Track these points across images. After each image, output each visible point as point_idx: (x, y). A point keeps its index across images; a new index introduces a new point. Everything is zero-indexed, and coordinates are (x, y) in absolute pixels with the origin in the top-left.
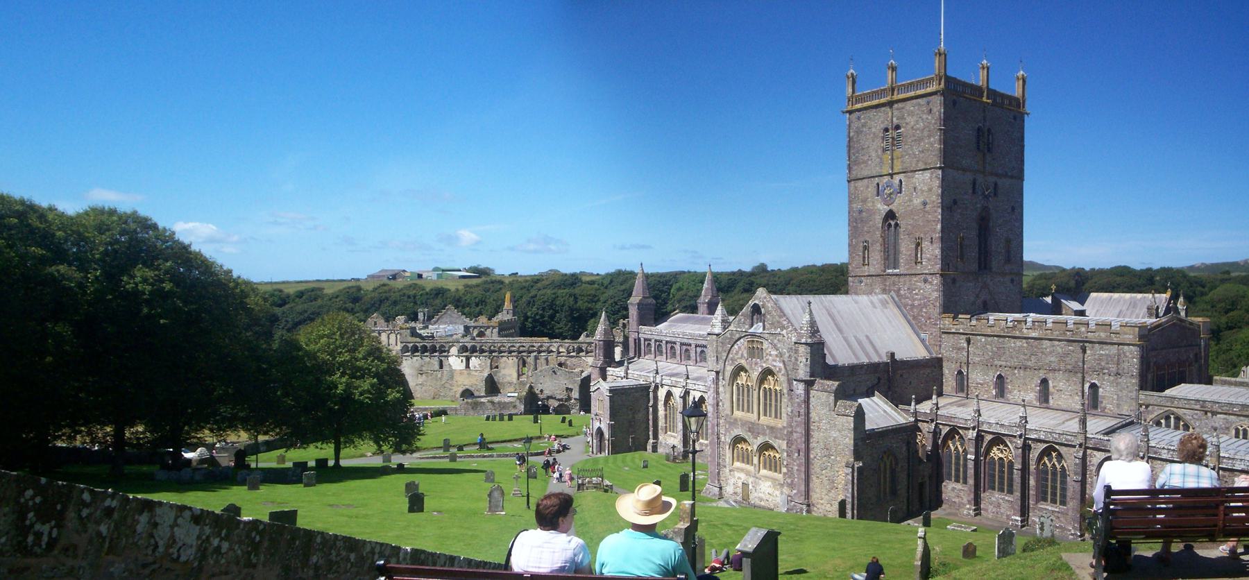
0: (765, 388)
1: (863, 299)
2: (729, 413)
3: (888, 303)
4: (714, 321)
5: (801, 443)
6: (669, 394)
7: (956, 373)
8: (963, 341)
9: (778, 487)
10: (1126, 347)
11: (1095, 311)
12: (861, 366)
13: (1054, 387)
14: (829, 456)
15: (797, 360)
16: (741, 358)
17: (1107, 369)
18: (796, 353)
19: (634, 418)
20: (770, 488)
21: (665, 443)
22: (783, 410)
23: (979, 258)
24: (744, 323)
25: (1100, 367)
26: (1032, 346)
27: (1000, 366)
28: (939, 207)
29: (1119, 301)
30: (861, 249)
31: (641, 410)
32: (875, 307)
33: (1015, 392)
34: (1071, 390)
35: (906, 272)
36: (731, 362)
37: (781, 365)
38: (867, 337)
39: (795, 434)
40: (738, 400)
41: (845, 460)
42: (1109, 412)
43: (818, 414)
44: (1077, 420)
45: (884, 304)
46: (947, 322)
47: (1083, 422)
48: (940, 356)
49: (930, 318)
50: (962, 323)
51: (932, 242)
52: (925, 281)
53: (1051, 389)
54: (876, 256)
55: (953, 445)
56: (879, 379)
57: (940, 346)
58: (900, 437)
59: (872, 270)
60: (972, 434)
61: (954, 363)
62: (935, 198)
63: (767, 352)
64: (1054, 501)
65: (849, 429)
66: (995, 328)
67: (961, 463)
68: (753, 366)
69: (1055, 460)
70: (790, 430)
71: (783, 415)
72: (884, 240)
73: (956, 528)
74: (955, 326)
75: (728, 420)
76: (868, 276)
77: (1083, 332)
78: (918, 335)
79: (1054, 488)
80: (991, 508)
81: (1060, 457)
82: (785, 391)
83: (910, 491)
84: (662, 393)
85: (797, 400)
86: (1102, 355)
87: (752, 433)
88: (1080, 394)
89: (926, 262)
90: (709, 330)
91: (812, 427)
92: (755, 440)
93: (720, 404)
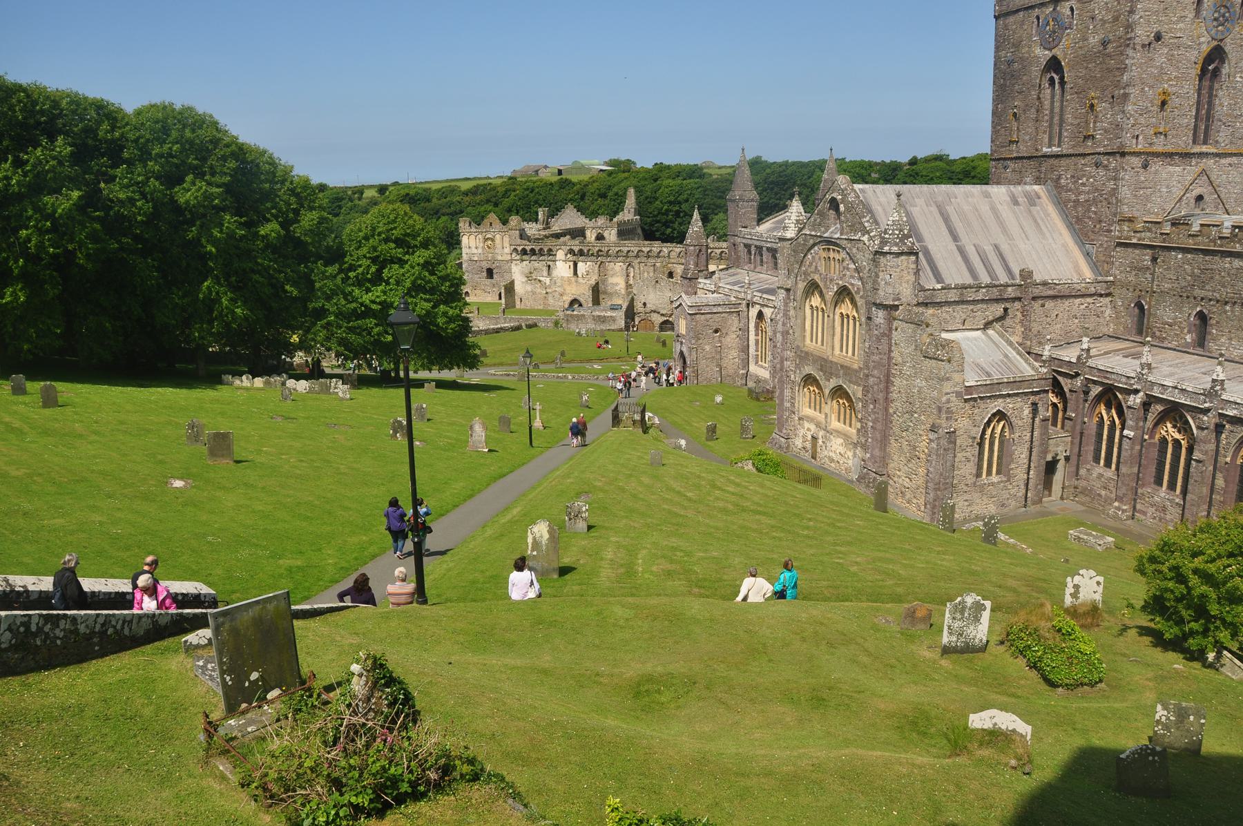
0: (841, 313)
1: (998, 192)
3: (1039, 198)
4: (787, 221)
6: (760, 315)
7: (1133, 305)
14: (911, 413)
15: (877, 276)
16: (815, 273)
20: (841, 448)
24: (820, 225)
27: (1202, 299)
32: (1016, 203)
35: (1071, 151)
36: (803, 277)
38: (996, 247)
39: (871, 380)
41: (931, 421)
43: (901, 354)
45: (1032, 200)
46: (1126, 228)
48: (1112, 278)
49: (1100, 221)
50: (1150, 230)
52: (1097, 165)
55: (1108, 414)
56: (1006, 310)
59: (1024, 150)
61: (1131, 290)
63: (845, 264)
66: (1200, 238)
67: (1117, 440)
73: (1081, 536)
74: (1138, 235)
75: (799, 353)
76: (1016, 158)
80: (1151, 510)
83: (1031, 473)
84: (753, 312)
85: (876, 332)
87: (825, 373)
89: (1100, 134)
90: (780, 234)
91: (894, 371)
92: (827, 383)
93: (791, 331)
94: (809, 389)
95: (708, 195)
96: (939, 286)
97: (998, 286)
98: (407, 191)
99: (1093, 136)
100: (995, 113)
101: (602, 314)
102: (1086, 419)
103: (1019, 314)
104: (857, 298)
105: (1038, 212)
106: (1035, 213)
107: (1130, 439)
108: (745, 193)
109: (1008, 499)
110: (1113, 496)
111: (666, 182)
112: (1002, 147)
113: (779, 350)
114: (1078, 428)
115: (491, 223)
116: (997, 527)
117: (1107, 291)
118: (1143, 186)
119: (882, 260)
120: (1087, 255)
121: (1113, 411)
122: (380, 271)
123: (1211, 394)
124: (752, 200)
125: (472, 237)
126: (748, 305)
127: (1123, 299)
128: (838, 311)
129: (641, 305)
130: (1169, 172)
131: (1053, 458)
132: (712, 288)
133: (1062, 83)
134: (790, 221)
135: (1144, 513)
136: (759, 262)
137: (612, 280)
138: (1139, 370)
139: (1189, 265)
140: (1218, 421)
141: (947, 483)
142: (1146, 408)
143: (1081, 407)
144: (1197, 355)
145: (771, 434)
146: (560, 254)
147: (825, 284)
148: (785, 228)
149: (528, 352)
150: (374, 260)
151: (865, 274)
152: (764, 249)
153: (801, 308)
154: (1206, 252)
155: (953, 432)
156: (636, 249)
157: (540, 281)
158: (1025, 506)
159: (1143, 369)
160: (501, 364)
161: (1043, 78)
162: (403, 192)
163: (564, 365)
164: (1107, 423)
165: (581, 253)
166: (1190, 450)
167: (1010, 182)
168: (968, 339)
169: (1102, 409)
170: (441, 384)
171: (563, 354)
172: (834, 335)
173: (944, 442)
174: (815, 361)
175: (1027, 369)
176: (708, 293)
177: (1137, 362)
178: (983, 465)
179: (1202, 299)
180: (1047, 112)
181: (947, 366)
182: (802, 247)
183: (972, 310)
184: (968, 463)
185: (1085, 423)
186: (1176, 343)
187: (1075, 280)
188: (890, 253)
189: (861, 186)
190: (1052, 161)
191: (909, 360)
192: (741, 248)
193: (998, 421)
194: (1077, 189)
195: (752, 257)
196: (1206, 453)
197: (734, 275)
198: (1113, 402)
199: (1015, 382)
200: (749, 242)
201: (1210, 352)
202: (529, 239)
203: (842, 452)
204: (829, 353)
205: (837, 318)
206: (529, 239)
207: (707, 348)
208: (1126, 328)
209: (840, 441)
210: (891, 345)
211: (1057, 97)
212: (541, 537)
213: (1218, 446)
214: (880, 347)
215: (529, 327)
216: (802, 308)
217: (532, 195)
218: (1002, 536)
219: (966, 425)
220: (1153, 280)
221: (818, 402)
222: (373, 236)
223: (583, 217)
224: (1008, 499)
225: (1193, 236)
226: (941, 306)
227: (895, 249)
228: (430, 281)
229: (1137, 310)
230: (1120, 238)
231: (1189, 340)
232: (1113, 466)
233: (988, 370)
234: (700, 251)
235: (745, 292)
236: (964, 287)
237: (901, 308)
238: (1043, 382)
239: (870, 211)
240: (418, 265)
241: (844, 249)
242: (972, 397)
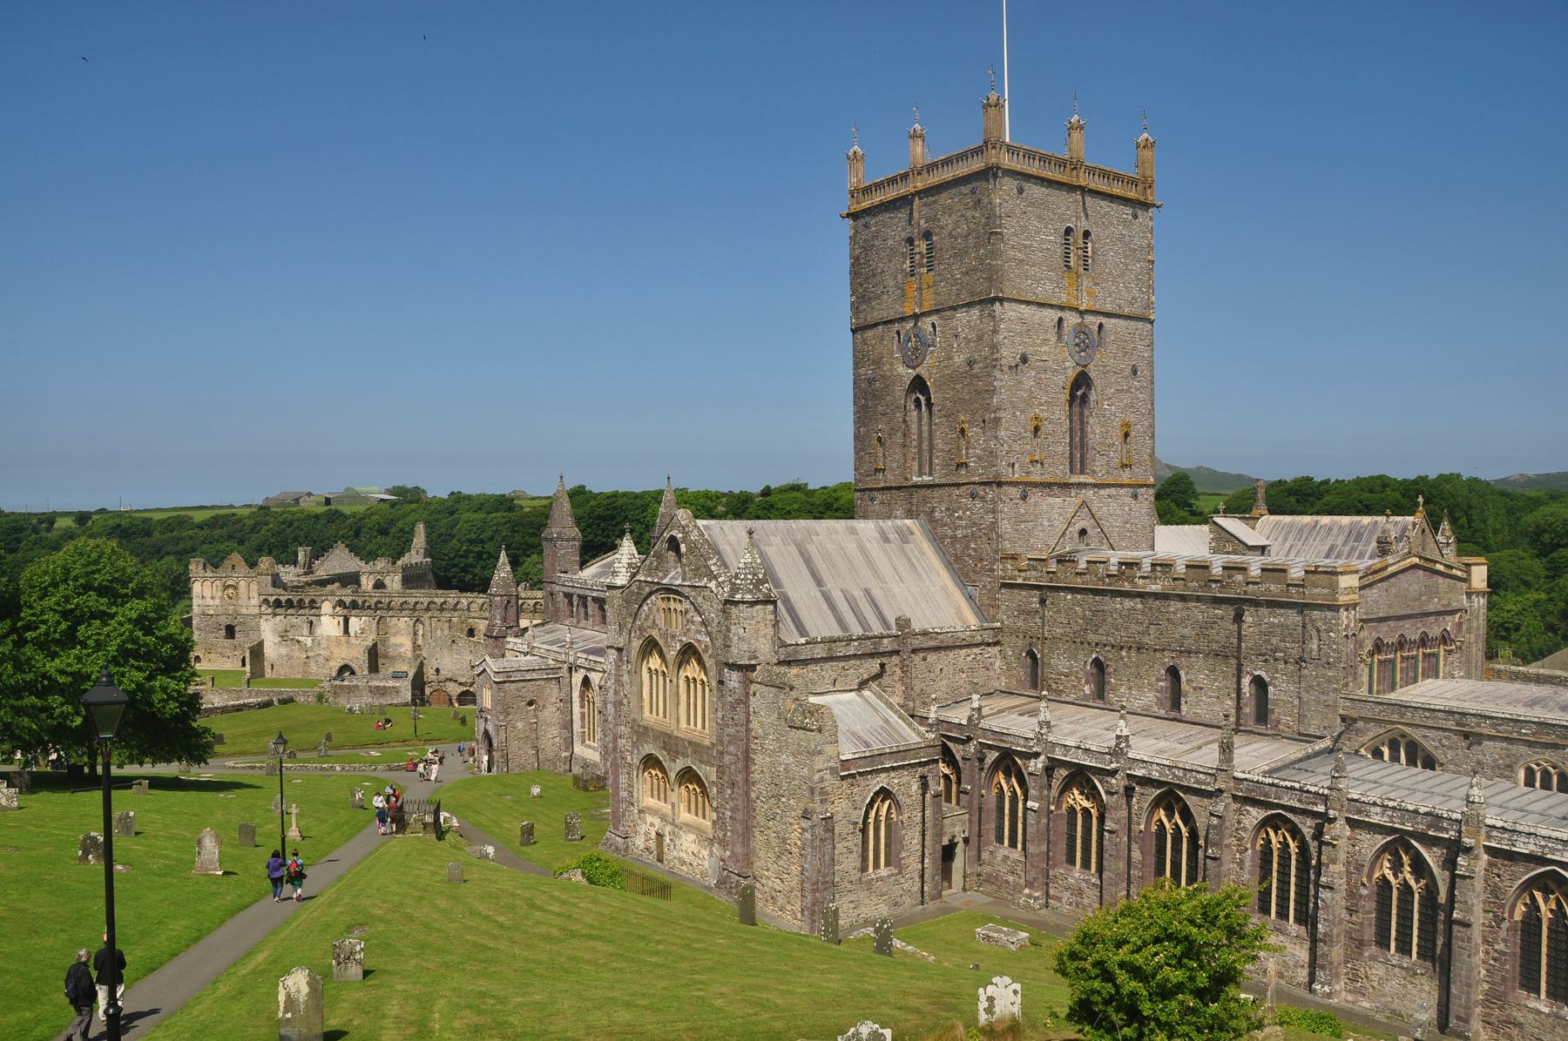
0: (687, 677)
1: (865, 527)
3: (912, 533)
4: (616, 565)
6: (586, 682)
7: (1024, 655)
11: (1287, 545)
13: (1187, 680)
14: (778, 797)
15: (729, 630)
16: (652, 628)
19: (536, 716)
24: (657, 569)
26: (1151, 609)
27: (1097, 644)
28: (995, 366)
29: (1330, 529)
32: (886, 540)
33: (1122, 690)
34: (1219, 689)
35: (943, 481)
36: (638, 632)
38: (867, 592)
39: (727, 759)
40: (651, 694)
44: (1216, 746)
45: (905, 536)
47: (1226, 749)
48: (999, 624)
49: (981, 560)
50: (1035, 569)
52: (973, 496)
53: (1184, 686)
55: (1008, 783)
56: (882, 666)
59: (891, 479)
60: (1037, 765)
61: (1021, 637)
63: (688, 616)
67: (1020, 814)
69: (1177, 816)
73: (991, 934)
74: (1023, 574)
75: (636, 728)
76: (884, 489)
77: (1239, 583)
80: (1066, 895)
81: (1187, 816)
83: (926, 861)
84: (577, 678)
85: (730, 699)
86: (1272, 625)
88: (1234, 695)
89: (974, 462)
90: (608, 581)
91: (753, 746)
93: (625, 701)
94: (650, 773)
95: (518, 531)
96: (803, 640)
97: (871, 638)
98: (117, 521)
99: (966, 463)
100: (857, 437)
101: (382, 684)
102: (983, 792)
103: (898, 671)
104: (705, 657)
105: (912, 550)
106: (908, 551)
107: (1035, 811)
108: (565, 529)
109: (901, 896)
110: (1022, 881)
111: (465, 516)
112: (867, 476)
113: (611, 726)
114: (976, 802)
115: (234, 566)
116: (891, 933)
117: (995, 639)
118: (1024, 519)
119: (734, 610)
120: (970, 598)
121: (1013, 780)
122: (73, 629)
123: (1116, 752)
124: (574, 539)
125: (208, 584)
126: (570, 669)
127: (1013, 647)
128: (682, 674)
129: (433, 671)
132: (525, 648)
133: (929, 405)
134: (621, 565)
135: (1059, 899)
136: (583, 615)
137: (394, 640)
138: (1037, 730)
139: (1079, 606)
140: (1127, 783)
141: (827, 882)
142: (1049, 773)
143: (977, 776)
144: (1098, 708)
145: (605, 833)
146: (327, 607)
147: (666, 642)
148: (615, 574)
149: (281, 736)
150: (65, 615)
151: (713, 628)
152: (589, 599)
153: (637, 672)
154: (1096, 592)
155: (829, 818)
156: (426, 601)
157: (298, 642)
158: (922, 903)
160: (243, 753)
161: (908, 399)
162: (111, 522)
163: (330, 753)
164: (1008, 794)
165: (354, 605)
166: (1101, 819)
167: (878, 517)
168: (840, 702)
169: (1001, 777)
170: (157, 783)
171: (329, 737)
172: (678, 704)
173: (819, 831)
174: (656, 738)
175: (911, 735)
176: (519, 654)
177: (1035, 720)
178: (868, 856)
179: (1097, 644)
180: (915, 437)
181: (817, 736)
182: (636, 597)
183: (843, 668)
184: (850, 856)
185: (983, 796)
186: (1074, 696)
187: (959, 628)
188: (744, 602)
189: (705, 522)
190: (923, 492)
191: (772, 731)
192: (561, 597)
193: (883, 801)
194: (954, 523)
195: (575, 609)
196: (1118, 822)
197: (552, 632)
198: (1013, 769)
199: (899, 752)
200: (571, 590)
202: (284, 587)
204: (674, 727)
205: (682, 682)
206: (284, 587)
207: (520, 725)
208: (1019, 681)
209: (692, 837)
210: (749, 714)
211: (925, 420)
212: (298, 991)
213: (1130, 813)
214: (736, 717)
215: (283, 702)
216: (638, 671)
217: (289, 530)
218: (898, 943)
219: (845, 807)
220: (1043, 626)
221: (662, 789)
222: (65, 581)
223: (357, 559)
224: (901, 896)
225: (1081, 574)
226: (807, 665)
227: (748, 597)
228: (146, 645)
229: (1029, 660)
230: (1004, 578)
231: (1088, 692)
232: (1020, 846)
233: (867, 739)
234: (509, 602)
235: (566, 654)
236: (833, 641)
237: (758, 668)
238: (931, 750)
239: (718, 552)
240: (130, 620)
241: (687, 598)
242: (849, 773)
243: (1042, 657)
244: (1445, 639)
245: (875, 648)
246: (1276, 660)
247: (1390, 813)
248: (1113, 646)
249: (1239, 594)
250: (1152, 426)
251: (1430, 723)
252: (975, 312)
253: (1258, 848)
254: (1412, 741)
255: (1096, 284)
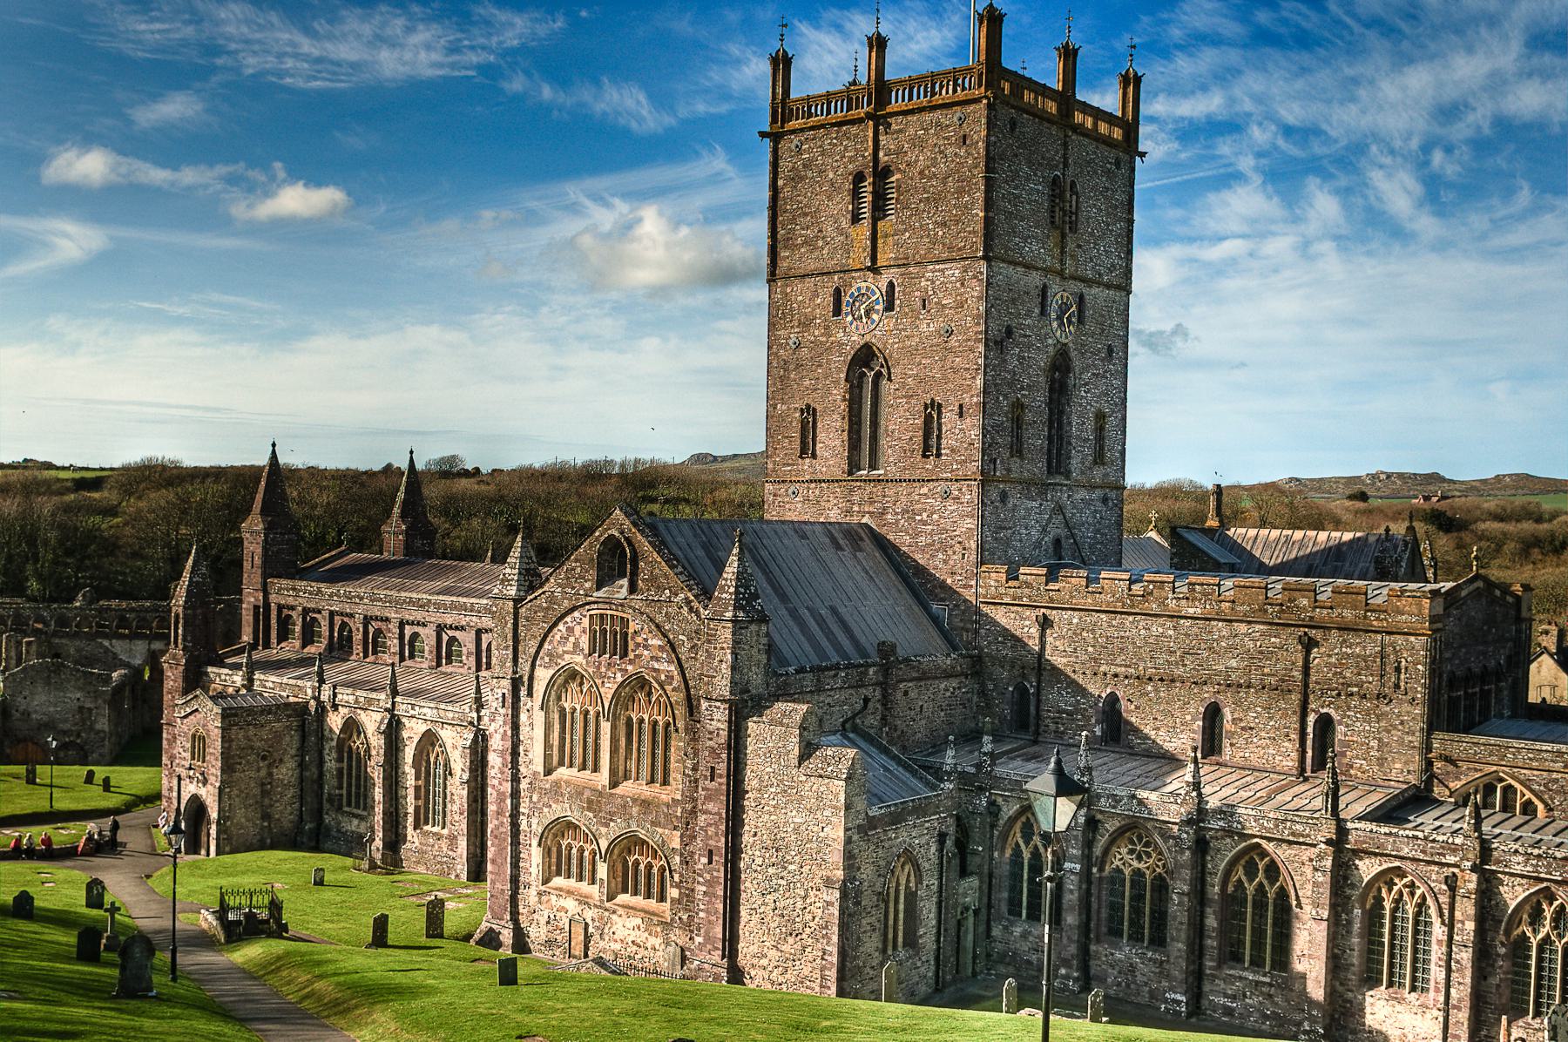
2: (540, 769)
3: (862, 539)
5: (717, 834)
6: (352, 726)
8: (1027, 623)
9: (659, 929)
10: (1400, 639)
12: (837, 667)
15: (710, 655)
16: (571, 653)
17: (1356, 686)
18: (709, 642)
19: (270, 774)
21: (339, 831)
22: (673, 765)
23: (1049, 451)
25: (1341, 680)
26: (1187, 635)
27: (1116, 675)
30: (797, 425)
31: (286, 758)
32: (839, 547)
37: (672, 668)
38: (834, 610)
39: (702, 819)
42: (1359, 774)
46: (992, 583)
47: (1334, 795)
51: (961, 415)
52: (947, 495)
53: (1228, 726)
54: (831, 438)
55: (1027, 843)
56: (866, 700)
57: (976, 632)
58: (927, 825)
62: (971, 326)
63: (639, 640)
64: (1257, 963)
65: (835, 807)
68: (603, 670)
70: (689, 807)
71: (672, 775)
72: (850, 407)
78: (926, 608)
79: (1259, 934)
81: (1273, 870)
82: (680, 724)
84: (335, 721)
87: (596, 813)
88: (1293, 736)
92: (603, 830)
96: (791, 669)
112: (788, 465)
120: (936, 620)
130: (1027, 509)
131: (962, 913)
159: (1083, 775)
164: (1026, 855)
185: (992, 858)
190: (869, 488)
200: (291, 601)
201: (1132, 748)
203: (638, 941)
231: (1099, 733)
236: (821, 669)
243: (1038, 688)
244: (1498, 675)
245: (861, 680)
246: (1352, 694)
247: (1534, 862)
248: (1138, 678)
249: (1303, 620)
250: (1124, 418)
251: (1535, 764)
252: (954, 271)
253: (1368, 907)
254: (1510, 786)
255: (1079, 246)
